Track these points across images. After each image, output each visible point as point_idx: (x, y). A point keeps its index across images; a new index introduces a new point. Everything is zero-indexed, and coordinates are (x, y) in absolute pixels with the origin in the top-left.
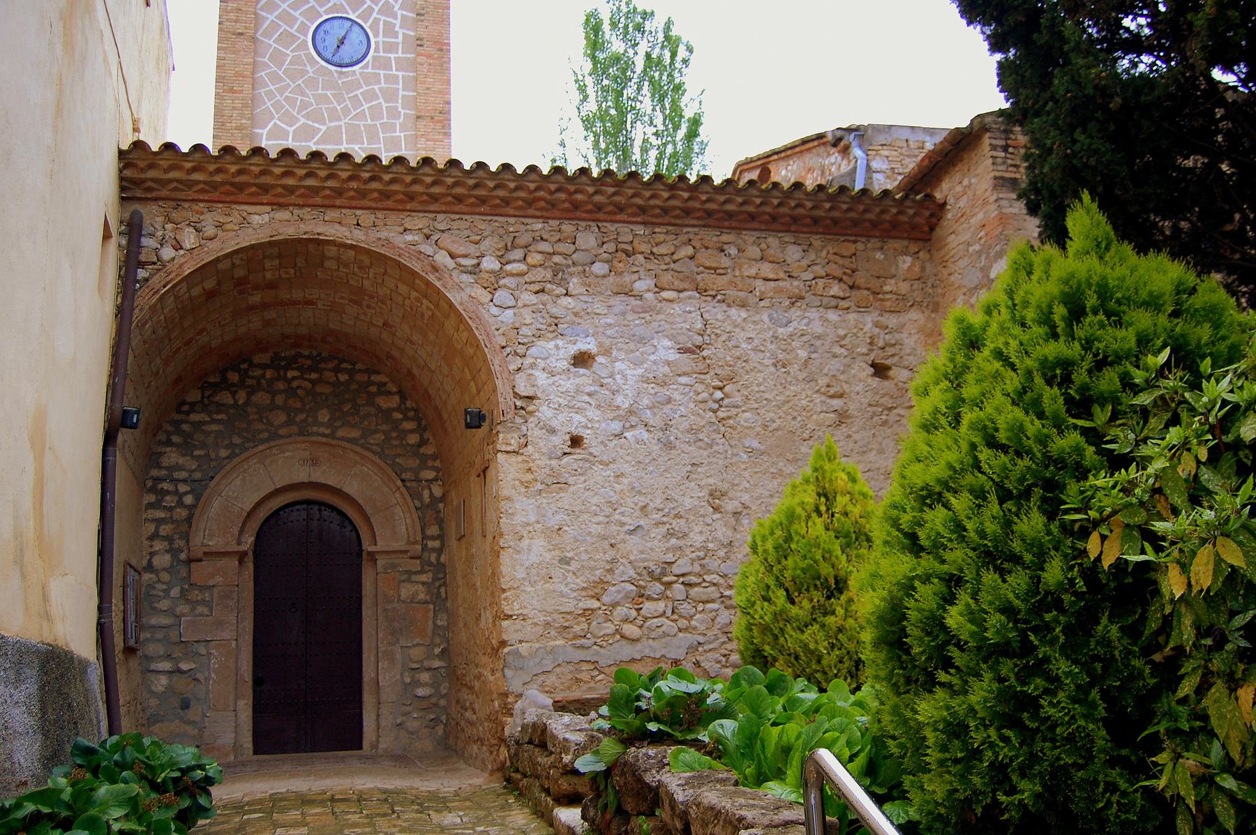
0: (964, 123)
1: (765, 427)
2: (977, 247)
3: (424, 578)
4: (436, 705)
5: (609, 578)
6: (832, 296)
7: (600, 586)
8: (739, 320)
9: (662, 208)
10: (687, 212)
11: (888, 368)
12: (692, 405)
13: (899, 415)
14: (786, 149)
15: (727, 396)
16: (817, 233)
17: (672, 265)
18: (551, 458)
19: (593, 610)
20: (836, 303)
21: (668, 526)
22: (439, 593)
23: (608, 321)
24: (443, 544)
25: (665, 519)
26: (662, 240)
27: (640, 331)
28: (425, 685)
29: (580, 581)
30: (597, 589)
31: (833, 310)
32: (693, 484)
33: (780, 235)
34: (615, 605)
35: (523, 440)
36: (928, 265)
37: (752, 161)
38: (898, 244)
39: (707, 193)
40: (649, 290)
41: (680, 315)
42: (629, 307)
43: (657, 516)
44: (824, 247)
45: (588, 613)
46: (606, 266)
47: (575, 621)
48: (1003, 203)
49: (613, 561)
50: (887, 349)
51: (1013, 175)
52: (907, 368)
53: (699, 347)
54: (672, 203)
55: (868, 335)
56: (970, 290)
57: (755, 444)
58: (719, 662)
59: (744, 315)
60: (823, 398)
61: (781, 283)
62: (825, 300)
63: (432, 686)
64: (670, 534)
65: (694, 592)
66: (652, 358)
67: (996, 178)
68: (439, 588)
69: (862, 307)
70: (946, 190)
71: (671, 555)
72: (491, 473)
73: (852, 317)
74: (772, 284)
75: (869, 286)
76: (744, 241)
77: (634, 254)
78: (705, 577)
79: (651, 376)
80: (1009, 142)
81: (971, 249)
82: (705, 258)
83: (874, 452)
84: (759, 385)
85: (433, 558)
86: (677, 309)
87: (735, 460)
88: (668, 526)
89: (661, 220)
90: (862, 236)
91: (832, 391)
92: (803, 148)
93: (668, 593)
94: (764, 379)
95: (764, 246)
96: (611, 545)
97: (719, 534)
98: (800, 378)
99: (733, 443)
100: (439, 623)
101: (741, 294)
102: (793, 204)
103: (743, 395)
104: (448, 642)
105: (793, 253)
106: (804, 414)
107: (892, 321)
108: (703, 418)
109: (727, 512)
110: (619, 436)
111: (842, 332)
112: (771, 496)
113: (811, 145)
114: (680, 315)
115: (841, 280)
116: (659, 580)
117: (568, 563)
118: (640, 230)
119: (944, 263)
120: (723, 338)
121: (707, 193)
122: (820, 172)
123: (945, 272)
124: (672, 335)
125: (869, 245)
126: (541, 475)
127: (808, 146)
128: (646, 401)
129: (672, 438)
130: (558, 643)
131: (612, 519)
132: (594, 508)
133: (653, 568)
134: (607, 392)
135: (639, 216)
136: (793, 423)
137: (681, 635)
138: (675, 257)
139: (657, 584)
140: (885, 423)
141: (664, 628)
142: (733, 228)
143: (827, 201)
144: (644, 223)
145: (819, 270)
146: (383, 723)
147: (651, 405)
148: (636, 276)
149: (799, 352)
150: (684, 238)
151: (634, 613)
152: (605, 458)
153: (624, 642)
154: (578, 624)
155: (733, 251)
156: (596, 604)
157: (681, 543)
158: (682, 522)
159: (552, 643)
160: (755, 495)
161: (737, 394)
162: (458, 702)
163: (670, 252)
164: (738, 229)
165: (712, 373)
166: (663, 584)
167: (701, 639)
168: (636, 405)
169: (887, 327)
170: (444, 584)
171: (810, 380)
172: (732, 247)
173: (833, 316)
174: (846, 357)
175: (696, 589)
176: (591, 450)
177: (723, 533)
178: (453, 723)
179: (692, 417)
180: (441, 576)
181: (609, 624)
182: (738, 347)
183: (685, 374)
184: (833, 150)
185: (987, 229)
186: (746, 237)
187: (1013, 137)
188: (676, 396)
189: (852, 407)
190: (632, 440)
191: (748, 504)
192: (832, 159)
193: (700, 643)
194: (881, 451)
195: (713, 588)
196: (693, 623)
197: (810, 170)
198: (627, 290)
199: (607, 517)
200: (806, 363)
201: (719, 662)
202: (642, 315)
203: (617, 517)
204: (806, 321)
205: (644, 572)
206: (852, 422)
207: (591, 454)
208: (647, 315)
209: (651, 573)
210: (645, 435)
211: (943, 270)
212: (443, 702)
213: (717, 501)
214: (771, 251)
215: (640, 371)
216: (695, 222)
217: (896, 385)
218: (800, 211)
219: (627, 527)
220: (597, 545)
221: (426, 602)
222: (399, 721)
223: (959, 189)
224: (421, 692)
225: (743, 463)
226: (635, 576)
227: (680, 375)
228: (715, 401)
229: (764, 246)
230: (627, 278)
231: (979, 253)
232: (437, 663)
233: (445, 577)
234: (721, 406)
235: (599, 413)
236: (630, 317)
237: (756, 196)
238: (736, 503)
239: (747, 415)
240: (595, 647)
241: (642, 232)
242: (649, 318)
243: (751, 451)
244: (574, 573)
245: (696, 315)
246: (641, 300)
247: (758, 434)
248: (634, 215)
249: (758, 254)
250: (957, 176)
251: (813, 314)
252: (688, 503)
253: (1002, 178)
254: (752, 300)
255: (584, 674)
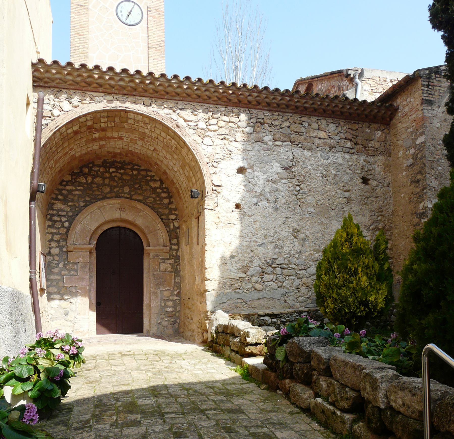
0: (411, 73)
1: (317, 203)
2: (411, 130)
3: (170, 261)
4: (175, 315)
5: (250, 265)
6: (347, 147)
7: (246, 268)
8: (308, 156)
9: (277, 104)
10: (287, 106)
11: (368, 180)
12: (287, 192)
13: (372, 201)
14: (322, 76)
15: (301, 189)
16: (342, 119)
17: (280, 130)
18: (227, 213)
19: (243, 278)
20: (348, 151)
21: (275, 244)
22: (177, 268)
23: (253, 153)
24: (179, 247)
25: (274, 241)
26: (276, 118)
27: (266, 159)
28: (170, 307)
29: (238, 266)
30: (245, 269)
31: (347, 154)
32: (286, 226)
33: (327, 119)
34: (252, 276)
35: (216, 204)
36: (388, 135)
37: (304, 79)
38: (376, 126)
39: (298, 98)
40: (270, 141)
41: (283, 153)
42: (262, 148)
43: (271, 239)
44: (345, 125)
45: (241, 279)
46: (252, 129)
47: (236, 282)
48: (425, 111)
49: (252, 257)
50: (369, 172)
51: (430, 99)
52: (376, 180)
53: (291, 167)
54: (282, 102)
55: (361, 165)
56: (406, 148)
57: (312, 210)
58: (294, 301)
59: (310, 154)
60: (341, 192)
61: (326, 140)
62: (344, 149)
63: (173, 307)
64: (276, 247)
65: (285, 271)
66: (271, 171)
67: (423, 99)
68: (177, 266)
69: (359, 153)
70: (400, 102)
71: (276, 256)
72: (201, 218)
73: (355, 157)
74: (322, 140)
75: (363, 144)
76: (311, 120)
77: (264, 124)
78: (290, 265)
79: (270, 179)
80: (430, 83)
81: (408, 130)
82: (295, 127)
83: (361, 216)
84: (315, 185)
85: (174, 253)
86: (282, 150)
87: (304, 216)
88: (275, 244)
89: (276, 109)
90: (361, 121)
91: (345, 189)
92: (330, 76)
93: (274, 271)
94: (317, 182)
95: (319, 123)
96: (252, 251)
97: (296, 248)
98: (332, 182)
99: (303, 209)
100: (177, 281)
101: (309, 144)
102: (334, 105)
103: (308, 189)
104: (180, 289)
105: (332, 127)
106: (333, 198)
107: (371, 159)
108: (291, 198)
109: (299, 239)
110: (256, 204)
111: (350, 163)
112: (318, 232)
113: (335, 75)
114: (283, 153)
115: (351, 140)
116: (271, 266)
117: (233, 258)
118: (267, 113)
119: (395, 135)
120: (301, 163)
121: (298, 98)
122: (338, 89)
123: (395, 139)
124: (280, 161)
125: (364, 125)
126: (223, 220)
127: (333, 76)
128: (267, 190)
129: (278, 206)
130: (229, 291)
131: (252, 240)
132: (245, 235)
133: (269, 261)
134: (251, 185)
135: (267, 107)
136: (328, 202)
137: (279, 289)
138: (282, 126)
139: (270, 268)
140: (366, 204)
141: (272, 286)
142: (307, 115)
143: (348, 105)
144: (269, 110)
145: (342, 135)
146: (152, 322)
147: (270, 191)
148: (265, 134)
149: (332, 171)
150: (285, 118)
151: (260, 279)
152: (250, 214)
153: (256, 291)
154: (237, 283)
155: (306, 125)
156: (244, 275)
157: (280, 251)
158: (281, 242)
159: (226, 291)
160: (311, 232)
161: (306, 188)
162: (184, 314)
163: (279, 124)
164: (309, 115)
165: (295, 179)
166: (272, 268)
167: (287, 291)
168: (263, 191)
169: (369, 162)
170: (179, 264)
171: (336, 184)
172: (306, 123)
173: (347, 156)
174: (351, 174)
175: (286, 270)
176: (244, 210)
177: (297, 247)
178: (182, 323)
179: (287, 198)
180: (178, 261)
181: (250, 284)
182: (307, 168)
183: (284, 179)
184: (345, 79)
185: (417, 122)
186: (312, 119)
187: (432, 81)
188: (280, 188)
189: (353, 196)
190: (261, 206)
191: (308, 235)
192: (344, 83)
193: (286, 293)
194: (363, 216)
195: (293, 270)
196: (284, 284)
197: (333, 87)
198: (261, 140)
199: (250, 239)
200: (335, 176)
201: (294, 301)
202: (267, 152)
203: (254, 239)
204: (336, 157)
205: (265, 263)
206: (353, 203)
207: (244, 212)
208: (269, 151)
209: (268, 263)
210: (267, 204)
211: (394, 138)
212: (177, 314)
213: (296, 234)
214: (322, 126)
215: (265, 176)
216: (291, 111)
217: (371, 187)
218: (337, 108)
219: (258, 243)
220: (246, 250)
221: (171, 272)
222: (159, 322)
223: (405, 103)
224: (169, 309)
225: (307, 218)
226: (261, 264)
227: (282, 179)
228: (296, 191)
229: (319, 123)
230: (261, 135)
231: (412, 133)
232: (176, 298)
233: (179, 261)
234: (299, 193)
235: (248, 194)
236: (262, 152)
237: (318, 101)
238: (303, 235)
239: (309, 198)
240: (244, 293)
241: (268, 114)
242: (269, 153)
243: (310, 213)
244: (236, 262)
245: (290, 153)
246: (267, 145)
247: (314, 206)
248: (265, 106)
249: (317, 127)
250: (405, 98)
251: (339, 155)
252: (284, 234)
253: (425, 99)
254: (314, 147)
255: (239, 304)
